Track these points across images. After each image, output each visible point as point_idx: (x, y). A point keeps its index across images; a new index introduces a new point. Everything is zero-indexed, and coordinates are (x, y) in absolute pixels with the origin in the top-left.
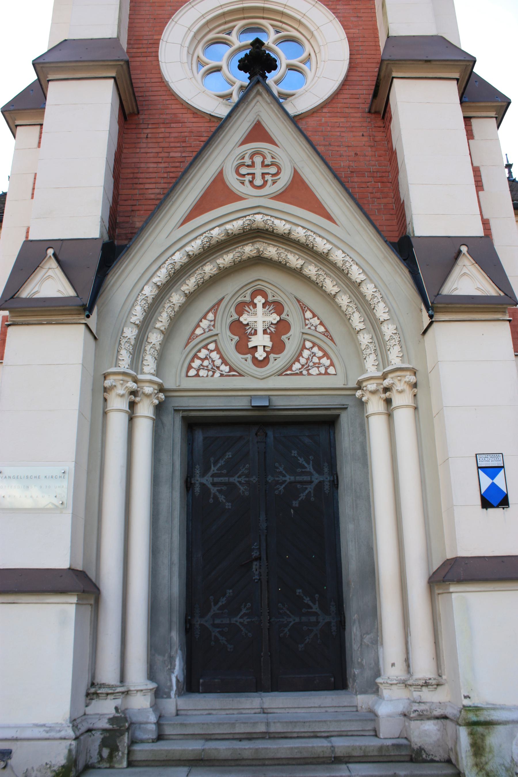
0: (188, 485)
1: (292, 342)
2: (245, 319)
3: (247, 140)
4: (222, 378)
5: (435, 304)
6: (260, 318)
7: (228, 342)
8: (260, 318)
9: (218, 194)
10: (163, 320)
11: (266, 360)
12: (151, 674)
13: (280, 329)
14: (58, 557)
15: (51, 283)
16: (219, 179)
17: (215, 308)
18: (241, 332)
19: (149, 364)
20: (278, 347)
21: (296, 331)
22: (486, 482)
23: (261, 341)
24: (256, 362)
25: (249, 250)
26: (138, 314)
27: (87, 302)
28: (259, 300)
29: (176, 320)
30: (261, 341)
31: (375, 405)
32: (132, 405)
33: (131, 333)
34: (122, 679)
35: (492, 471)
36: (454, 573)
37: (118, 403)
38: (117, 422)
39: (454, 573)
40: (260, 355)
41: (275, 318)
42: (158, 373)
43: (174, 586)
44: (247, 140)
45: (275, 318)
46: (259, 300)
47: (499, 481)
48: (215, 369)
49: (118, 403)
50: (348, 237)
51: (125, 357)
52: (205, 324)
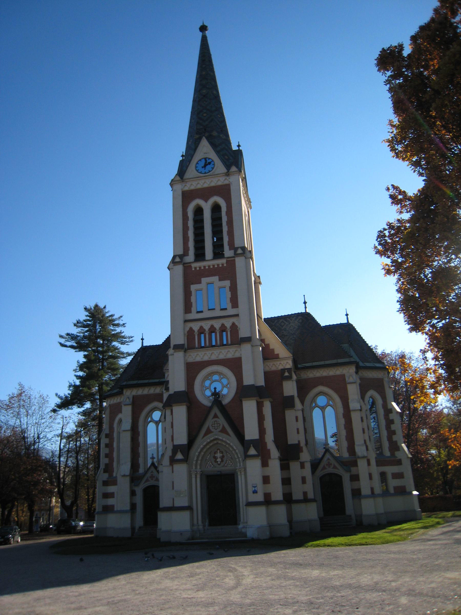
1: (225, 460)
2: (216, 455)
5: (247, 456)
6: (219, 455)
7: (213, 460)
8: (219, 455)
10: (200, 458)
11: (220, 464)
12: (203, 522)
13: (222, 458)
14: (186, 504)
15: (179, 456)
16: (208, 428)
17: (210, 453)
18: (215, 458)
19: (198, 467)
20: (222, 461)
21: (225, 457)
22: (254, 489)
23: (219, 460)
24: (218, 464)
25: (215, 442)
26: (195, 459)
27: (186, 460)
28: (218, 451)
29: (202, 458)
30: (219, 460)
31: (239, 473)
32: (196, 475)
33: (194, 462)
34: (198, 523)
35: (255, 487)
36: (250, 504)
37: (193, 476)
38: (194, 479)
39: (250, 504)
40: (219, 463)
41: (221, 455)
42: (200, 469)
45: (221, 455)
46: (218, 451)
47: (256, 489)
48: (210, 466)
49: (193, 476)
50: (232, 440)
51: (194, 467)
52: (208, 457)
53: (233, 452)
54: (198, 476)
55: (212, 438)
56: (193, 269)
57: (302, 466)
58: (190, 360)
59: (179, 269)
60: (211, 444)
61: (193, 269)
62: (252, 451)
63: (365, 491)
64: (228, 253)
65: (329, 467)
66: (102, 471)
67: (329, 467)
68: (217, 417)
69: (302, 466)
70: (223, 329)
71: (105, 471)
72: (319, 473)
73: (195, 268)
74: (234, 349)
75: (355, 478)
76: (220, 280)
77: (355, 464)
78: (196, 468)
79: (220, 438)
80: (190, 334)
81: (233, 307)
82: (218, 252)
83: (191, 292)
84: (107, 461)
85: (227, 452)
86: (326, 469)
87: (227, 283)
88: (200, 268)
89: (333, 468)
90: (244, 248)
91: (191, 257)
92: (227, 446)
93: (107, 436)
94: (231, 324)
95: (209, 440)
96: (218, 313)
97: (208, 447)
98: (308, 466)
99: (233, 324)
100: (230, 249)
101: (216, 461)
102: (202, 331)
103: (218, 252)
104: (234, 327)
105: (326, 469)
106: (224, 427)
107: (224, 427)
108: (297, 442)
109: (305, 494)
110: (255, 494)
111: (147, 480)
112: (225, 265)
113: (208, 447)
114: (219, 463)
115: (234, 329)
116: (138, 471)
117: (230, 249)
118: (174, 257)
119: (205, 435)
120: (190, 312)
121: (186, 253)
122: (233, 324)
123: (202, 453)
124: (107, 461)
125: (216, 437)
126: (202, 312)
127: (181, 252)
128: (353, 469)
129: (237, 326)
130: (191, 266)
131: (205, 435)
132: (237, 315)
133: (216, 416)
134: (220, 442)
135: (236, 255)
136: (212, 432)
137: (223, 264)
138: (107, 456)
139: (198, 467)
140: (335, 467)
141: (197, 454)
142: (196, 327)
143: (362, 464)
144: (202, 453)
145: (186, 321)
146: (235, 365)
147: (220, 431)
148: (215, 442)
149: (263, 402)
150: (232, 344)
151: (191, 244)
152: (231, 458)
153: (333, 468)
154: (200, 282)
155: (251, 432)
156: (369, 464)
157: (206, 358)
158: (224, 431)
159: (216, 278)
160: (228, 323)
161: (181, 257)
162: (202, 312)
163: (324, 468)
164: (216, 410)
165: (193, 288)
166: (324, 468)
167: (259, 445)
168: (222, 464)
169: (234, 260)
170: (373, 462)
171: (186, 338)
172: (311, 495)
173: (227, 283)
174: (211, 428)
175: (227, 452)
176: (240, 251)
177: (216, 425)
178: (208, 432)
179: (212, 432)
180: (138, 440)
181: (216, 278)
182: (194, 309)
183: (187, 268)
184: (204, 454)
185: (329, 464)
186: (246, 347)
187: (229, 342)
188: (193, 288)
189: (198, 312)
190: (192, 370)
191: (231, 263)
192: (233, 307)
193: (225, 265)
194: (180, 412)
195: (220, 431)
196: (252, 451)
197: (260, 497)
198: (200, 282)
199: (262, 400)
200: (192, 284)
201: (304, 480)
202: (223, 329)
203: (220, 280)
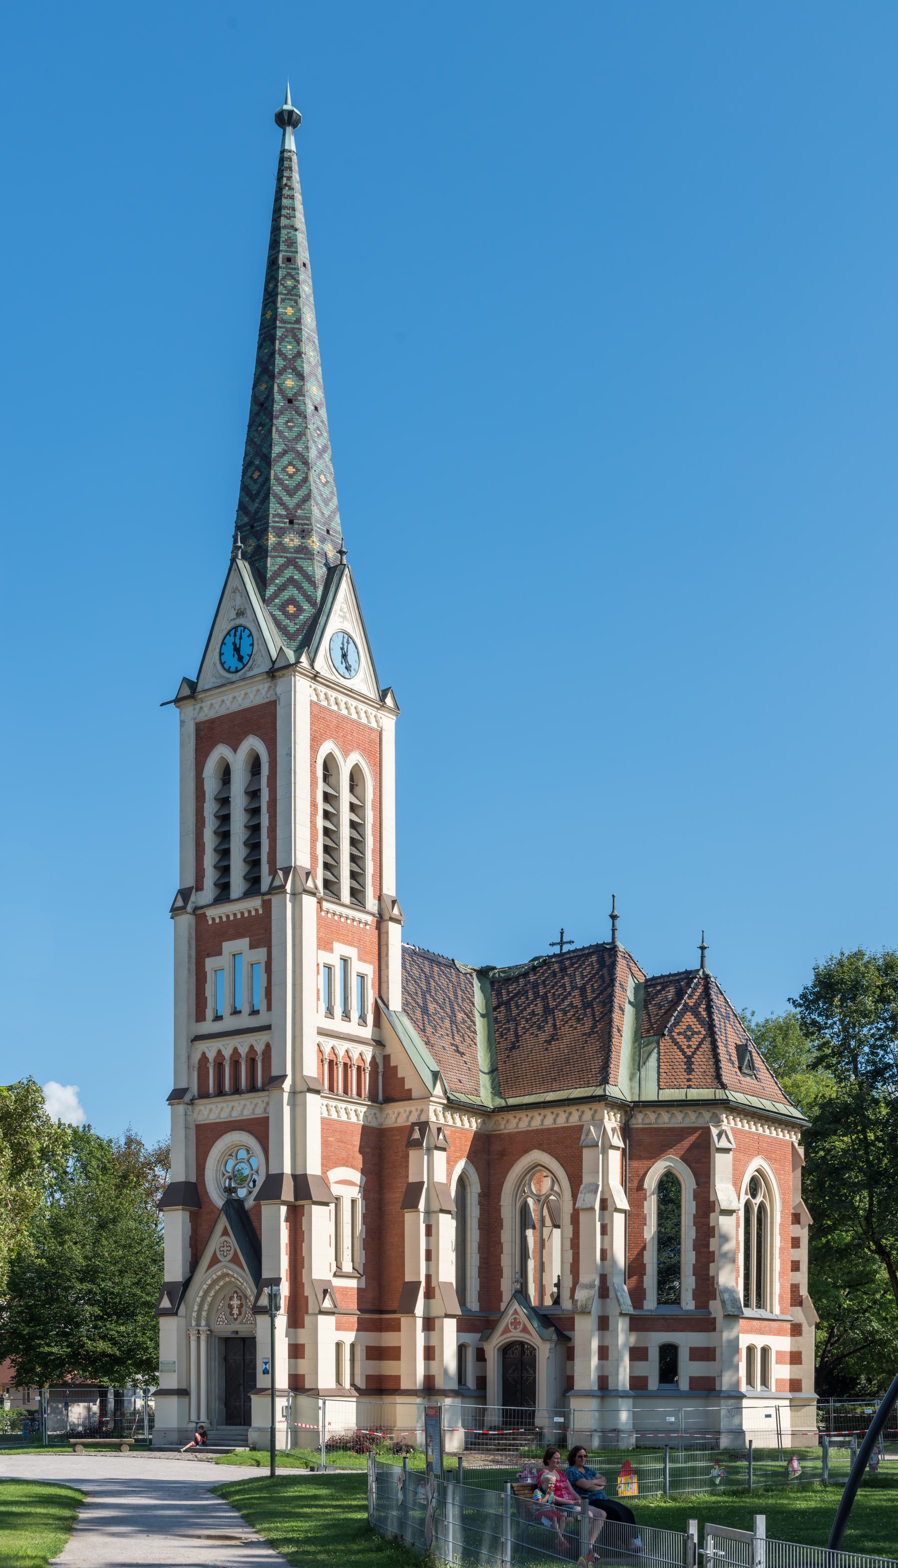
1: (243, 1313)
2: (232, 1303)
3: (222, 1235)
4: (225, 1328)
6: (235, 1302)
10: (206, 1307)
16: (215, 1253)
17: (223, 1299)
18: (231, 1307)
19: (203, 1323)
20: (240, 1314)
23: (236, 1311)
30: (236, 1311)
37: (193, 1338)
40: (235, 1316)
41: (239, 1302)
45: (239, 1302)
54: (203, 1338)
56: (210, 922)
59: (186, 919)
61: (210, 922)
78: (198, 1324)
91: (208, 893)
114: (235, 1316)
130: (204, 915)
141: (198, 1299)
154: (220, 953)
157: (224, 1117)
165: (210, 963)
168: (240, 1318)
178: (215, 1261)
182: (209, 1014)
188: (210, 963)
198: (220, 953)
200: (209, 956)
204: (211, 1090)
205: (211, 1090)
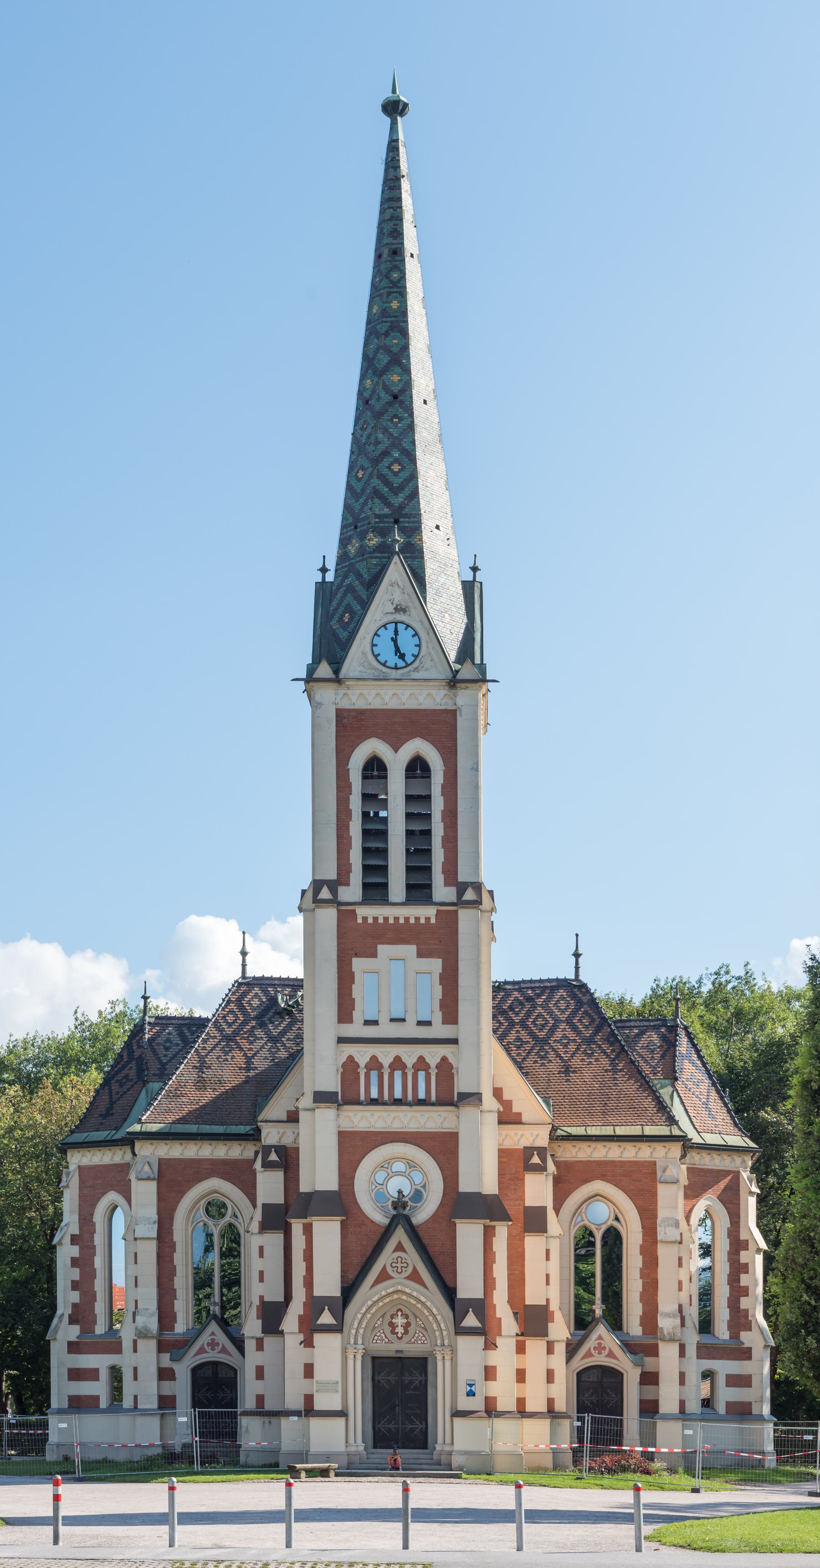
0: (373, 1379)
3: (395, 1250)
6: (400, 1321)
8: (400, 1321)
9: (384, 1276)
17: (383, 1316)
22: (469, 1388)
25: (396, 1296)
38: (350, 1363)
39: (457, 1414)
43: (370, 1413)
44: (395, 1250)
53: (431, 1318)
55: (391, 1290)
56: (360, 921)
57: (550, 1350)
58: (347, 1126)
59: (328, 916)
60: (388, 1300)
61: (360, 921)
62: (471, 1320)
63: (668, 1403)
64: (442, 892)
65: (600, 1353)
66: (66, 1319)
67: (600, 1353)
68: (405, 1251)
69: (550, 1350)
70: (421, 1064)
71: (73, 1320)
72: (580, 1362)
73: (365, 919)
74: (444, 1114)
75: (650, 1379)
76: (420, 955)
77: (653, 1351)
79: (408, 1290)
80: (349, 1068)
81: (445, 1021)
82: (419, 890)
83: (352, 976)
84: (75, 1297)
85: (416, 1317)
86: (592, 1356)
87: (435, 965)
88: (375, 919)
89: (608, 1356)
90: (478, 887)
91: (352, 892)
92: (419, 1306)
93: (74, 1240)
94: (439, 1060)
95: (384, 1293)
96: (410, 1030)
97: (381, 1304)
98: (560, 1349)
99: (444, 1059)
100: (447, 884)
101: (393, 1332)
102: (374, 1064)
103: (419, 890)
104: (445, 1066)
105: (592, 1356)
106: (415, 1270)
107: (415, 1270)
108: (544, 1303)
109: (550, 1402)
110: (471, 1398)
111: (201, 1351)
112: (433, 921)
113: (381, 1304)
114: (400, 1335)
115: (446, 1069)
116: (173, 1329)
117: (447, 884)
118: (317, 885)
119: (377, 1282)
120: (351, 1021)
121: (343, 878)
122: (444, 1059)
123: (369, 1316)
124: (75, 1297)
125: (399, 1288)
126: (375, 1023)
127: (332, 875)
128: (649, 1360)
129: (451, 1067)
131: (377, 1282)
132: (455, 1041)
133: (400, 1247)
134: (404, 1297)
135: (460, 902)
136: (392, 1278)
137: (428, 919)
138: (75, 1286)
139: (360, 1341)
140: (611, 1355)
142: (362, 1055)
143: (668, 1353)
144: (369, 1316)
145: (341, 1040)
146: (444, 1148)
147: (408, 1278)
148: (396, 1296)
149: (494, 1227)
150: (440, 1102)
151: (356, 857)
152: (425, 1328)
153: (608, 1356)
154: (374, 955)
155: (469, 1285)
156: (682, 1353)
158: (415, 1277)
159: (412, 949)
160: (433, 1055)
161: (333, 886)
162: (375, 1023)
163: (589, 1354)
164: (400, 1235)
165: (358, 964)
166: (589, 1354)
167: (481, 1307)
168: (406, 1338)
169: (456, 912)
170: (691, 1350)
171: (339, 1076)
172: (560, 1406)
173: (435, 965)
174: (389, 1270)
175: (416, 1317)
176: (469, 895)
177: (399, 1265)
179: (392, 1278)
180: (172, 1260)
181: (412, 949)
183: (346, 915)
184: (362, 1318)
185: (600, 1348)
186: (467, 1112)
187: (433, 1098)
188: (358, 964)
189: (367, 1023)
190: (353, 1147)
191: (448, 921)
192: (445, 1021)
193: (433, 921)
194: (328, 1233)
195: (408, 1278)
196: (471, 1320)
197: (477, 1403)
198: (374, 955)
199: (493, 1223)
200: (356, 955)
201: (550, 1376)
202: (421, 1064)
203: (420, 955)
204: (362, 1097)
205: (362, 1097)
